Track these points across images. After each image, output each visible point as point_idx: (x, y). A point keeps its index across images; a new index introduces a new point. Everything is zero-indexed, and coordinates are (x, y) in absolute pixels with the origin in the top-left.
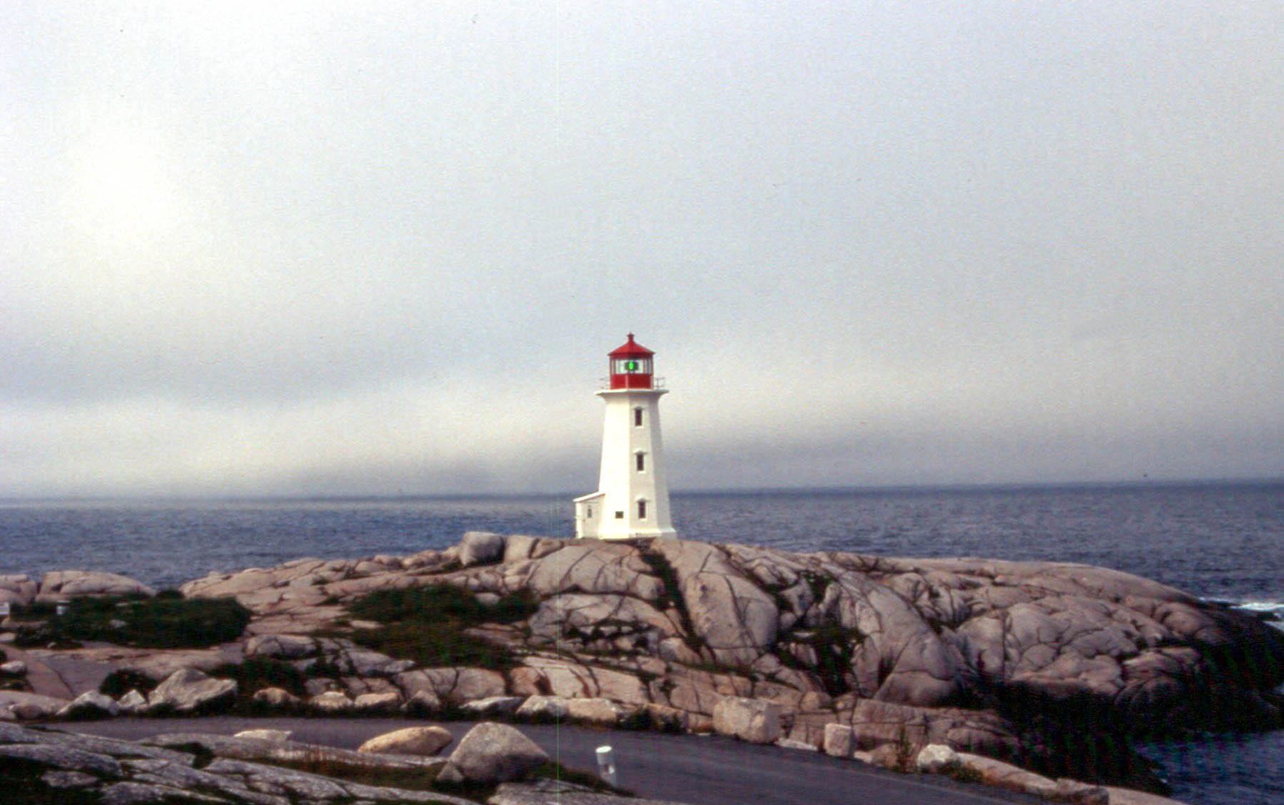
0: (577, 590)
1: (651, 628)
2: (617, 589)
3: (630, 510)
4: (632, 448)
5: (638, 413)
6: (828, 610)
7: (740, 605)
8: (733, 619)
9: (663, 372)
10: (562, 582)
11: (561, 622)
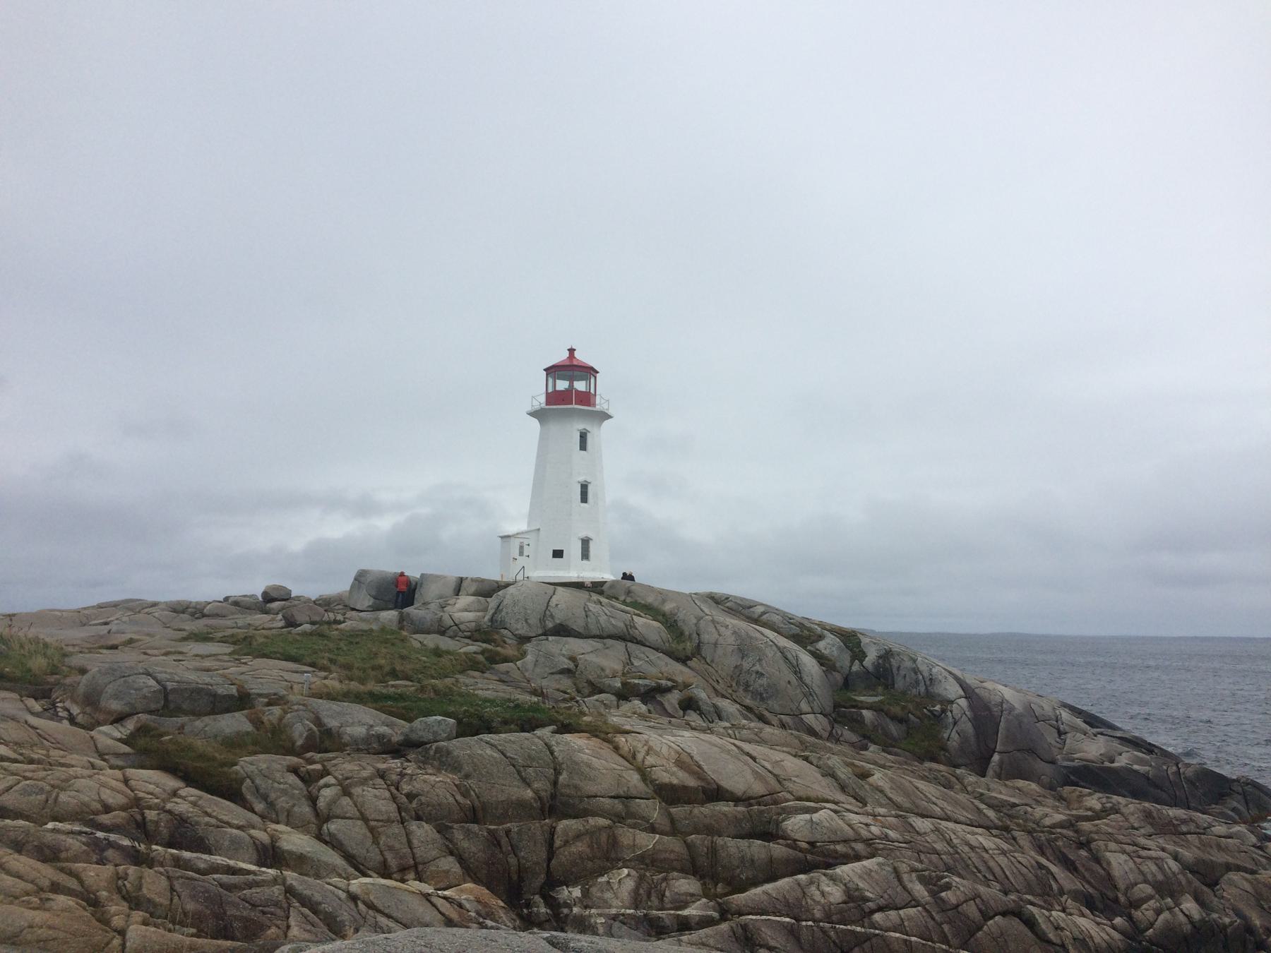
0: (562, 631)
1: (687, 686)
2: (613, 631)
3: (574, 550)
5: (583, 437)
6: (877, 666)
7: (789, 656)
8: (793, 678)
9: (605, 390)
10: (542, 620)
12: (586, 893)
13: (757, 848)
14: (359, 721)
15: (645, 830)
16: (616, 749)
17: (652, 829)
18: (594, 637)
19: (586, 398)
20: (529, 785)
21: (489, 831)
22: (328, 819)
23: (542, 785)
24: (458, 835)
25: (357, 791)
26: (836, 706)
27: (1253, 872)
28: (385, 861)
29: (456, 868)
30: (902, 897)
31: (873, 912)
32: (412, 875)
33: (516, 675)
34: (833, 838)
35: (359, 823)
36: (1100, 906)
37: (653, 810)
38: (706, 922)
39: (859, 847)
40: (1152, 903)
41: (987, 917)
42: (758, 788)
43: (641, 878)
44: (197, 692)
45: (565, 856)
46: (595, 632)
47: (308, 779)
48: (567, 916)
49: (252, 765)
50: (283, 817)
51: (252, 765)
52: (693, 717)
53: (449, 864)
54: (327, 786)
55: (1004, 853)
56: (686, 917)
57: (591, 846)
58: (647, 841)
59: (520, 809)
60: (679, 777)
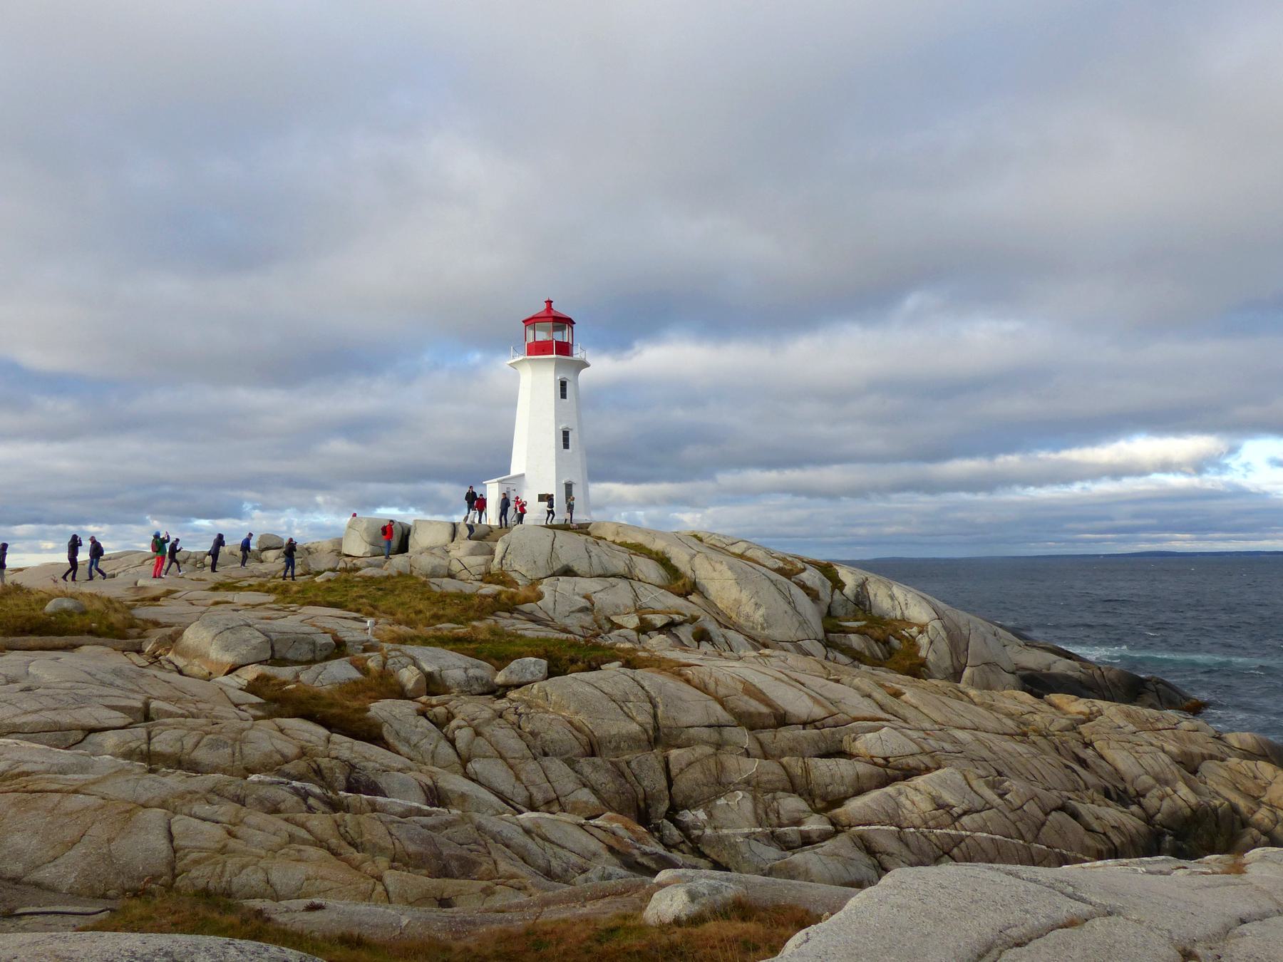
0: (568, 572)
1: (694, 619)
2: (615, 571)
4: (557, 423)
5: (563, 385)
6: (857, 595)
8: (787, 607)
11: (583, 610)
12: (710, 815)
13: (842, 767)
14: (453, 666)
15: (741, 754)
16: (688, 681)
17: (748, 754)
18: (599, 576)
19: (564, 349)
20: (633, 719)
21: (612, 763)
22: (469, 760)
23: (645, 718)
24: (587, 770)
25: (486, 730)
26: (827, 631)
27: (1223, 760)
28: (531, 796)
29: (593, 799)
30: (978, 803)
31: (960, 816)
32: (555, 808)
33: (541, 615)
34: (902, 752)
35: (500, 761)
36: (1114, 796)
37: (742, 737)
38: (825, 836)
39: (926, 759)
40: (1154, 791)
41: (1047, 814)
42: (818, 712)
43: (755, 798)
44: (296, 641)
45: (684, 783)
46: (600, 572)
47: (440, 724)
48: (699, 837)
49: (381, 709)
50: (428, 759)
51: (381, 709)
52: (705, 646)
53: (585, 795)
54: (459, 727)
55: (1035, 756)
56: (808, 832)
57: (703, 773)
58: (752, 767)
59: (633, 742)
60: (755, 706)
